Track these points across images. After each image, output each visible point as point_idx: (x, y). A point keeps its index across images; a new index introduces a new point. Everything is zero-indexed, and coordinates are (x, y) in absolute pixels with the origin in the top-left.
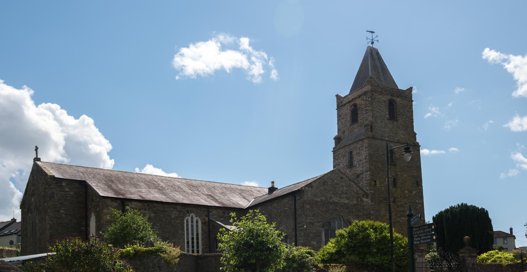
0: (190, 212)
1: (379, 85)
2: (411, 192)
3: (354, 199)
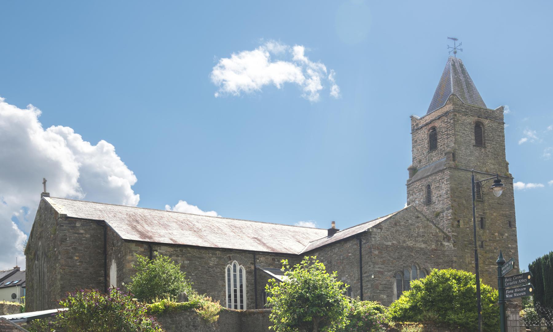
0: (232, 259)
1: (463, 104)
3: (433, 243)
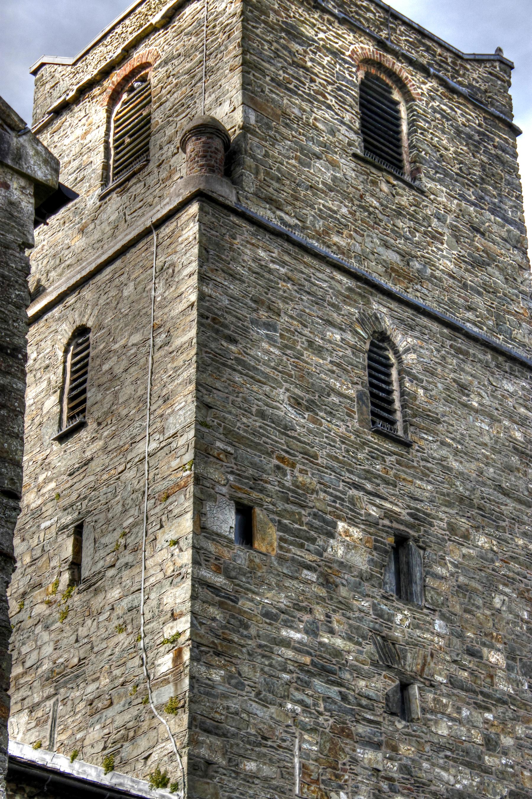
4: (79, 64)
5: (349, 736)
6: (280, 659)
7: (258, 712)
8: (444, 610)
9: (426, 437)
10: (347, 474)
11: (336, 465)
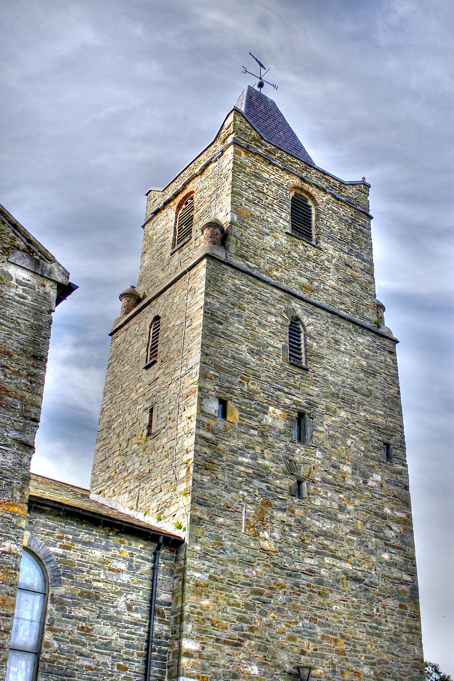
2: (366, 477)
4: (165, 191)
5: (270, 506)
6: (237, 471)
7: (225, 496)
8: (322, 447)
9: (316, 365)
10: (275, 384)
11: (270, 380)
